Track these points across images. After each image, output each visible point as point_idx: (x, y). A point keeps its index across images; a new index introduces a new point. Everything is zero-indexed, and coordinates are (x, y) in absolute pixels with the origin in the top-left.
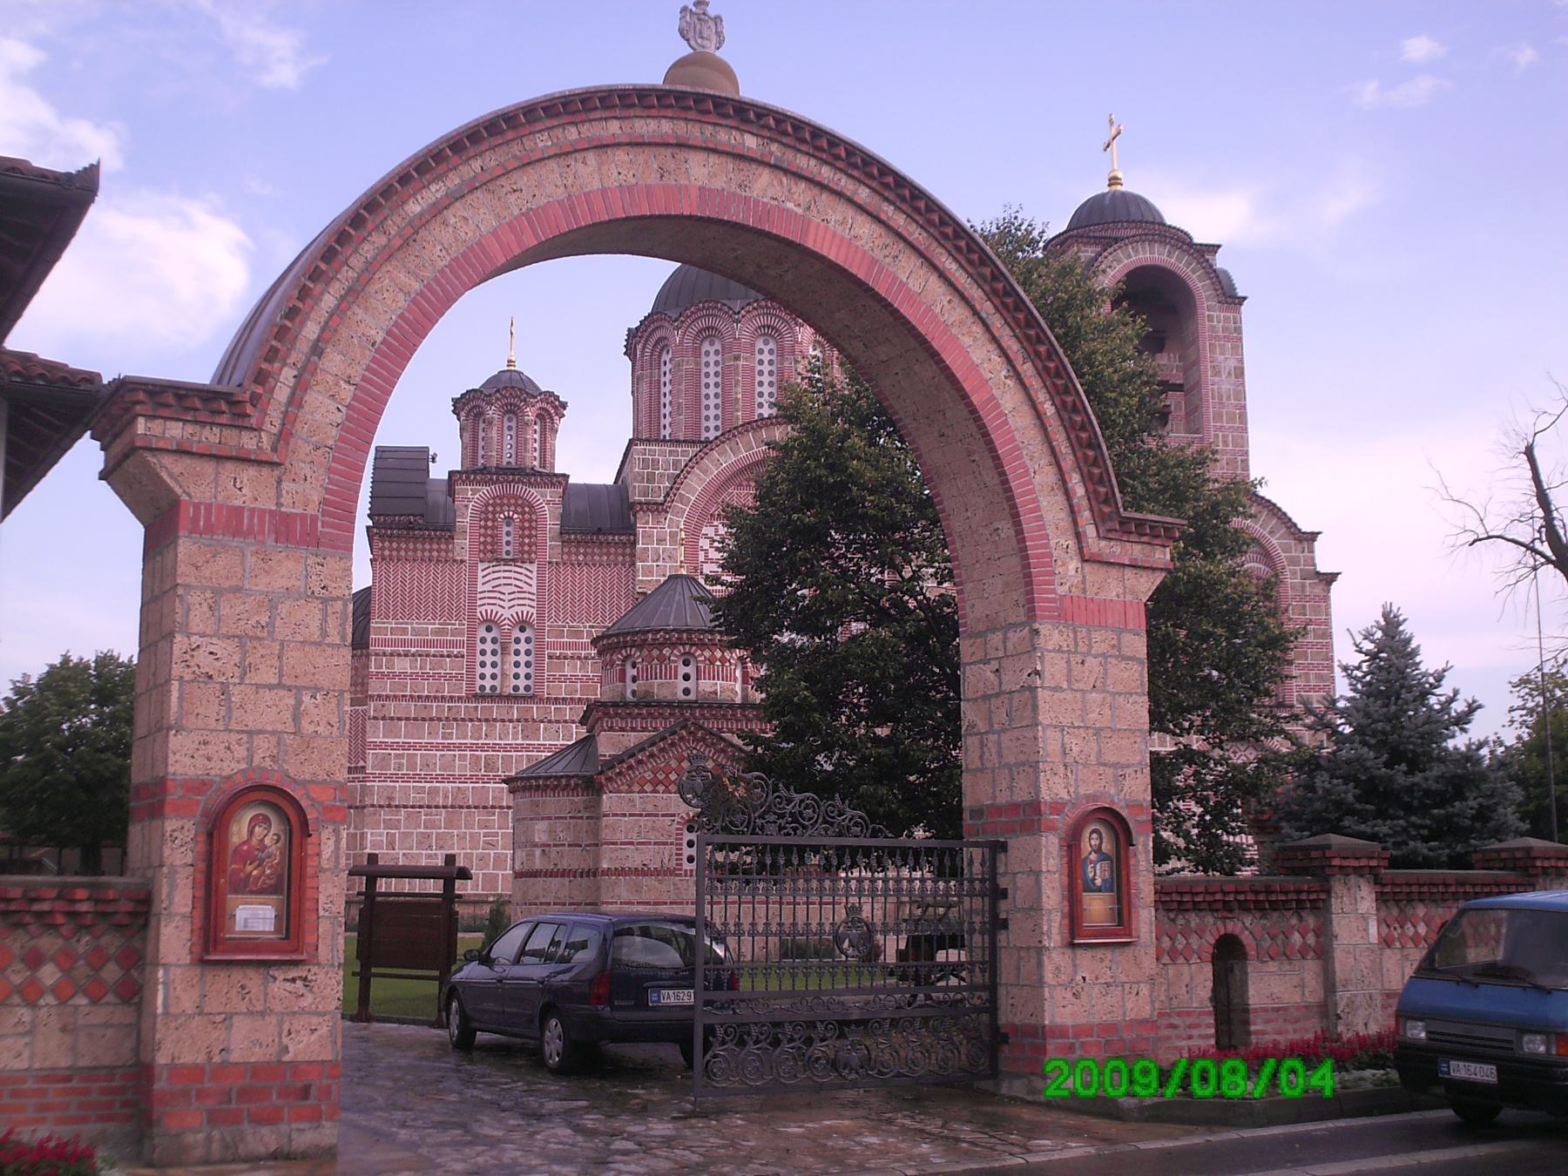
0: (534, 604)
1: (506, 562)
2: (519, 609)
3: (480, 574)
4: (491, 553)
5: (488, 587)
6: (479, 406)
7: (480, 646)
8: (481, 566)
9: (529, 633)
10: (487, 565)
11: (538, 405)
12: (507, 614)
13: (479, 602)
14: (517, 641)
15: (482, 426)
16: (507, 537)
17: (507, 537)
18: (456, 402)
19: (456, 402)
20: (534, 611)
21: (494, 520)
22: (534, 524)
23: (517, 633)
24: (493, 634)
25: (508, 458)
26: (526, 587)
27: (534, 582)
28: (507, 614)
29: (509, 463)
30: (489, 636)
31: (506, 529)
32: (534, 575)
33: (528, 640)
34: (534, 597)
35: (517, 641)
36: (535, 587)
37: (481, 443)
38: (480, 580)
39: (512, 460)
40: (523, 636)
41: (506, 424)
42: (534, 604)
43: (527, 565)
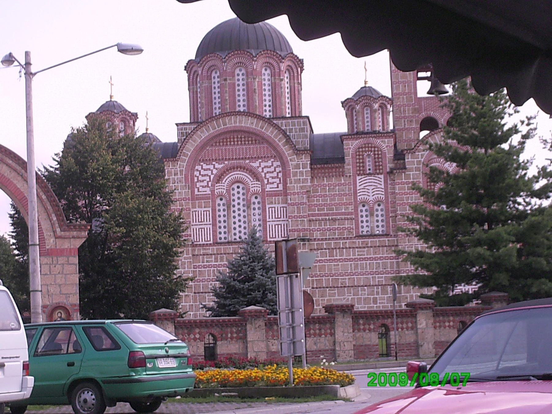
0: (383, 193)
1: (370, 174)
3: (358, 182)
4: (361, 171)
5: (362, 187)
7: (360, 214)
8: (358, 178)
10: (360, 177)
11: (381, 102)
12: (371, 198)
13: (358, 194)
14: (377, 210)
15: (354, 114)
16: (369, 164)
17: (369, 164)
18: (343, 103)
19: (343, 103)
20: (384, 196)
21: (363, 155)
22: (380, 156)
23: (376, 207)
24: (366, 207)
25: (368, 128)
26: (379, 186)
27: (383, 183)
28: (371, 198)
29: (368, 130)
30: (364, 209)
31: (368, 160)
32: (382, 180)
33: (382, 210)
36: (383, 185)
37: (355, 122)
38: (358, 184)
39: (369, 128)
41: (365, 112)
42: (383, 193)
43: (379, 176)
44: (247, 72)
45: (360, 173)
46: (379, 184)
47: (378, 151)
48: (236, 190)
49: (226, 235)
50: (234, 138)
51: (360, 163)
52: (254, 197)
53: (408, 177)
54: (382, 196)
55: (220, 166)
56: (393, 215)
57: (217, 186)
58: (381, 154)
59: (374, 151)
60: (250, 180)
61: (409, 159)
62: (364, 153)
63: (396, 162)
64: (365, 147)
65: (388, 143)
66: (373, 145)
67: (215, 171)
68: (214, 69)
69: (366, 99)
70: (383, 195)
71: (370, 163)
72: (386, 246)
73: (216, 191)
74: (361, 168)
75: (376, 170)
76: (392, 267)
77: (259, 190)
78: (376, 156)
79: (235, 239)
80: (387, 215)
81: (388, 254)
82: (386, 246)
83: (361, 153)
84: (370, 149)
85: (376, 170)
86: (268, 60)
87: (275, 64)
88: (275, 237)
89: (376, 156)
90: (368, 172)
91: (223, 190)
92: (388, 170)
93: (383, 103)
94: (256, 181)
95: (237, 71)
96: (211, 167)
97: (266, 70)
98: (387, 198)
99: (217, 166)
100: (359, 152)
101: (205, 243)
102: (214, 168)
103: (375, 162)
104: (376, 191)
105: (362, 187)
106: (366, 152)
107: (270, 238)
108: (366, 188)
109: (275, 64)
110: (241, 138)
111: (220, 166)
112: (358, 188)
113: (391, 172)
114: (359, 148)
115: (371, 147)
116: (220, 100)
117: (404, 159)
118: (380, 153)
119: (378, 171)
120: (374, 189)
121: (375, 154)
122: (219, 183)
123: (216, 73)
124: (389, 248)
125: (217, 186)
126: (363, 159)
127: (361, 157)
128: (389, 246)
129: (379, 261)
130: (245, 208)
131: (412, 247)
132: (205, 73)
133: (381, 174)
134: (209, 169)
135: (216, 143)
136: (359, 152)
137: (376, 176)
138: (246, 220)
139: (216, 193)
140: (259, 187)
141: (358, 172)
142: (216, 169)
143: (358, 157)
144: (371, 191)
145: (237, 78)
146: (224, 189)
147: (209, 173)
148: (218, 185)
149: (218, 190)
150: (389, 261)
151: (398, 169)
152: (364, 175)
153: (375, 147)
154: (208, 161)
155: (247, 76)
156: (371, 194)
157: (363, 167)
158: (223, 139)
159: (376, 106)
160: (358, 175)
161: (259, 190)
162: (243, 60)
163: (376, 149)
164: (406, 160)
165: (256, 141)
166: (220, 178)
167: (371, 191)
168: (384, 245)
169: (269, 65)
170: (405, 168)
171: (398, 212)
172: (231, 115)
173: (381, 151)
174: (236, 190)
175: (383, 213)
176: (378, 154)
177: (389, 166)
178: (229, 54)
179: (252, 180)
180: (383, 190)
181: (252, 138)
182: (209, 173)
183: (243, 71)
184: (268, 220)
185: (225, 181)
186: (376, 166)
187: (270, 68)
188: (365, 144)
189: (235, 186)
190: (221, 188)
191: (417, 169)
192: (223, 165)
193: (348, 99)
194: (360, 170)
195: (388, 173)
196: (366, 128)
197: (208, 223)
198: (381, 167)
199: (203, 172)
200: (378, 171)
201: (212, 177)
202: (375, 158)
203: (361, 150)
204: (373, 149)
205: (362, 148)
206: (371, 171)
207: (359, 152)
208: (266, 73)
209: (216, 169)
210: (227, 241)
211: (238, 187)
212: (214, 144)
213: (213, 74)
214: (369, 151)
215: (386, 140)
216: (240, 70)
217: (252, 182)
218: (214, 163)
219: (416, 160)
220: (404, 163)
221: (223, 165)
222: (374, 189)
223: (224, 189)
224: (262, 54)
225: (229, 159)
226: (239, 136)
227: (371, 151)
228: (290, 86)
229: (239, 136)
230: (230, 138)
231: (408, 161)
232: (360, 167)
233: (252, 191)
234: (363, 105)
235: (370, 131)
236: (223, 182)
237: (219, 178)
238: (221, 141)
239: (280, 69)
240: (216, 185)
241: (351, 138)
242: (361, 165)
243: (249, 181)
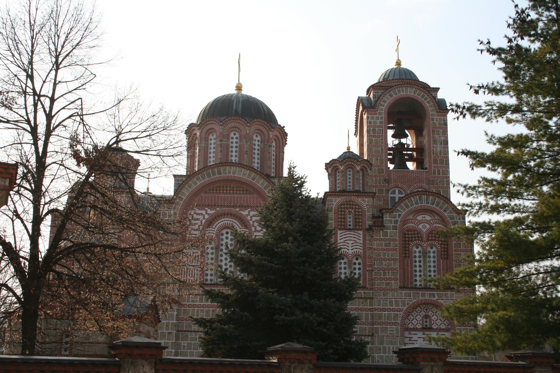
0: (362, 248)
1: (350, 229)
2: (355, 250)
3: (339, 235)
5: (342, 241)
6: (337, 166)
9: (360, 261)
10: (341, 232)
12: (350, 252)
14: (355, 264)
15: (338, 174)
16: (350, 220)
20: (362, 251)
21: (345, 212)
23: (355, 261)
26: (358, 241)
27: (361, 239)
28: (350, 252)
31: (349, 216)
32: (361, 236)
33: (359, 264)
34: (362, 245)
35: (355, 264)
38: (339, 238)
39: (351, 188)
40: (357, 262)
41: (348, 173)
43: (359, 232)
44: (240, 136)
45: (341, 228)
46: (358, 239)
47: (359, 209)
48: (225, 235)
50: (227, 187)
51: (341, 218)
53: (386, 234)
54: (360, 251)
55: (212, 212)
56: (370, 269)
58: (361, 212)
59: (355, 208)
60: (239, 227)
61: (387, 217)
62: (346, 209)
63: (374, 220)
64: (347, 204)
65: (368, 203)
66: (354, 203)
67: (207, 216)
68: (212, 132)
69: (350, 161)
70: (361, 249)
71: (351, 220)
72: (362, 298)
74: (343, 224)
75: (356, 226)
76: (367, 318)
78: (357, 213)
80: (364, 268)
81: (364, 306)
82: (362, 298)
83: (343, 210)
84: (351, 206)
85: (356, 226)
86: (259, 127)
87: (265, 131)
89: (357, 213)
90: (348, 227)
91: (212, 234)
92: (367, 227)
93: (364, 167)
94: (245, 228)
95: (232, 135)
96: (204, 212)
97: (257, 136)
98: (365, 252)
99: (209, 211)
100: (341, 208)
102: (206, 213)
103: (356, 219)
104: (355, 245)
105: (342, 241)
106: (347, 209)
108: (346, 242)
109: (265, 131)
110: (233, 187)
111: (212, 212)
112: (339, 241)
113: (370, 229)
114: (341, 205)
115: (353, 205)
116: (214, 159)
117: (383, 218)
118: (360, 210)
119: (358, 227)
120: (353, 243)
121: (355, 212)
122: (210, 228)
123: (213, 135)
124: (364, 300)
126: (344, 215)
127: (343, 213)
128: (365, 298)
129: (355, 312)
131: (387, 301)
132: (203, 136)
133: (361, 230)
134: (201, 214)
135: (210, 190)
136: (341, 208)
137: (356, 231)
141: (339, 227)
142: (208, 214)
143: (340, 213)
144: (350, 245)
145: (231, 140)
146: (214, 233)
147: (201, 217)
148: (209, 229)
150: (364, 312)
151: (377, 226)
152: (345, 230)
153: (356, 205)
154: (201, 206)
155: (240, 139)
156: (350, 248)
157: (344, 222)
158: (217, 187)
159: (358, 168)
160: (340, 230)
162: (238, 125)
163: (357, 207)
164: (385, 219)
165: (247, 191)
166: (211, 223)
167: (350, 245)
168: (360, 296)
169: (261, 133)
170: (384, 226)
171: (376, 267)
172: (226, 165)
173: (361, 208)
174: (225, 235)
175: (361, 266)
176: (359, 212)
177: (369, 223)
178: (226, 118)
179: (241, 227)
180: (362, 245)
181: (243, 188)
182: (201, 217)
183: (237, 135)
185: (215, 227)
186: (356, 222)
187: (260, 134)
188: (347, 201)
189: (224, 232)
190: (212, 232)
191: (395, 228)
192: (214, 211)
193: (333, 160)
194: (341, 225)
195: (367, 230)
196: (348, 188)
198: (360, 224)
199: (195, 216)
200: (358, 227)
201: (204, 221)
202: (355, 215)
203: (343, 206)
204: (354, 207)
205: (344, 205)
206: (351, 227)
207: (341, 208)
208: (257, 139)
209: (208, 214)
211: (227, 233)
212: (208, 192)
213: (211, 137)
214: (350, 208)
215: (366, 199)
216: (235, 134)
218: (206, 209)
219: (393, 219)
220: (382, 222)
221: (214, 211)
222: (353, 243)
223: (214, 233)
224: (255, 122)
225: (221, 206)
226: (232, 186)
227: (352, 208)
228: (276, 154)
229: (232, 186)
230: (223, 187)
231: (386, 220)
232: (341, 222)
234: (348, 165)
235: (352, 190)
236: (214, 227)
237: (210, 223)
238: (215, 189)
239: (269, 137)
241: (335, 195)
242: (343, 220)
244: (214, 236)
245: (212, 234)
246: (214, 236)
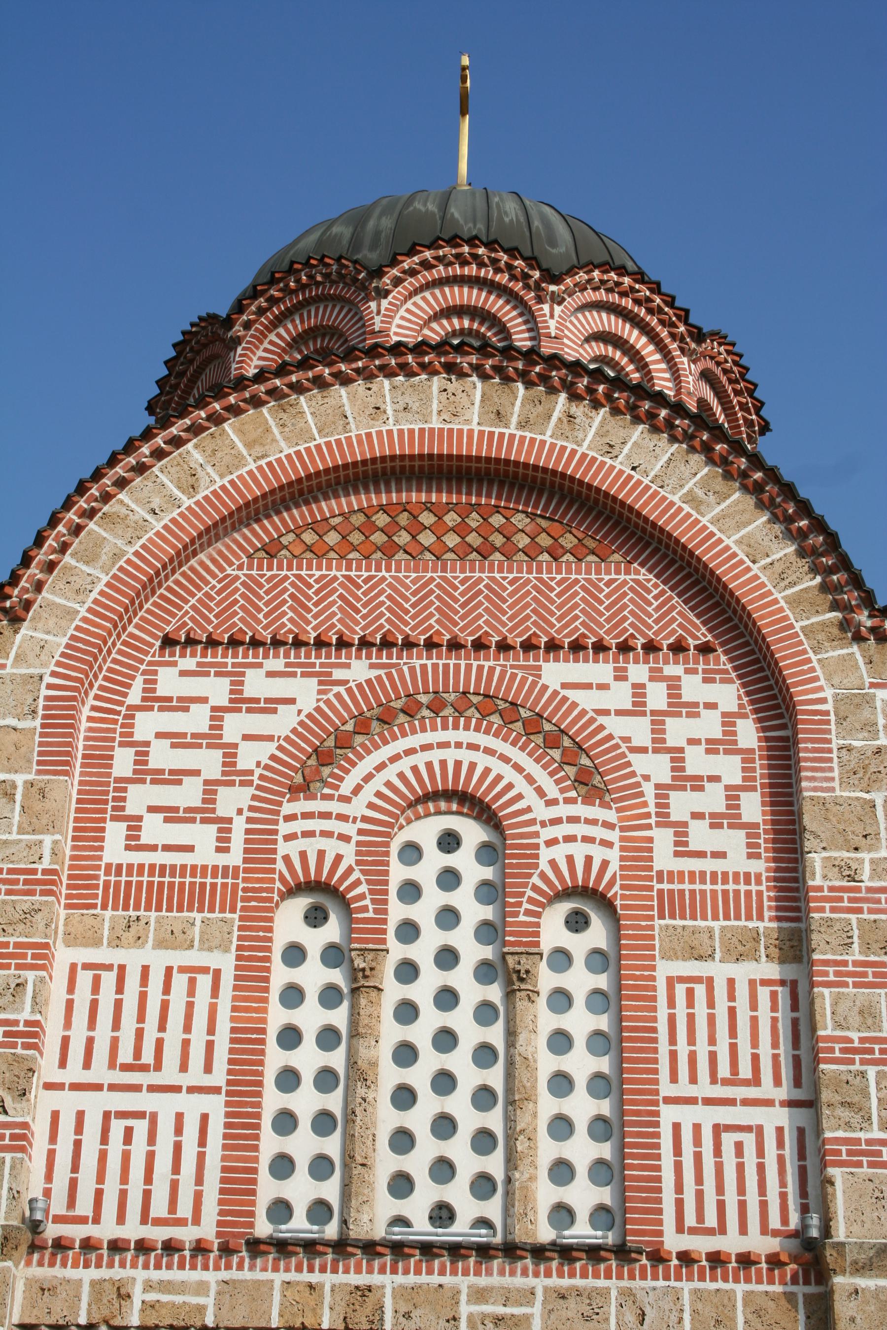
49: (330, 1190)
52: (565, 907)
57: (290, 818)
73: (283, 848)
77: (605, 864)
79: (401, 1221)
88: (722, 1229)
94: (588, 800)
101: (159, 1234)
107: (680, 1228)
125: (290, 818)
130: (494, 993)
138: (495, 1077)
139: (280, 865)
140: (607, 844)
149: (301, 844)
161: (605, 864)
179: (553, 791)
184: (666, 1089)
185: (357, 790)
197: (196, 1076)
210: (331, 1231)
217: (552, 802)
233: (553, 863)
236: (346, 788)
240: (288, 808)
243: (531, 798)
244: (349, 859)
245: (332, 847)
246: (349, 852)
